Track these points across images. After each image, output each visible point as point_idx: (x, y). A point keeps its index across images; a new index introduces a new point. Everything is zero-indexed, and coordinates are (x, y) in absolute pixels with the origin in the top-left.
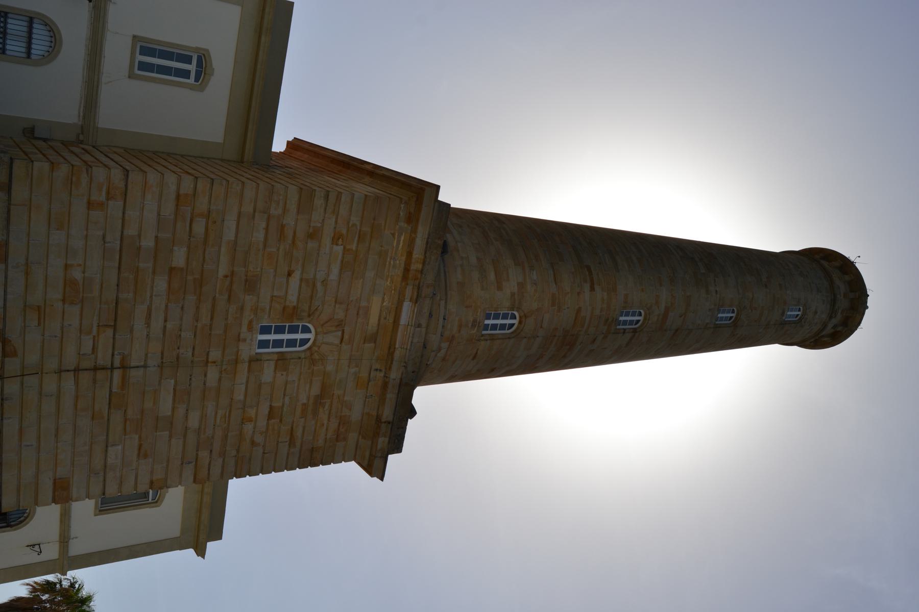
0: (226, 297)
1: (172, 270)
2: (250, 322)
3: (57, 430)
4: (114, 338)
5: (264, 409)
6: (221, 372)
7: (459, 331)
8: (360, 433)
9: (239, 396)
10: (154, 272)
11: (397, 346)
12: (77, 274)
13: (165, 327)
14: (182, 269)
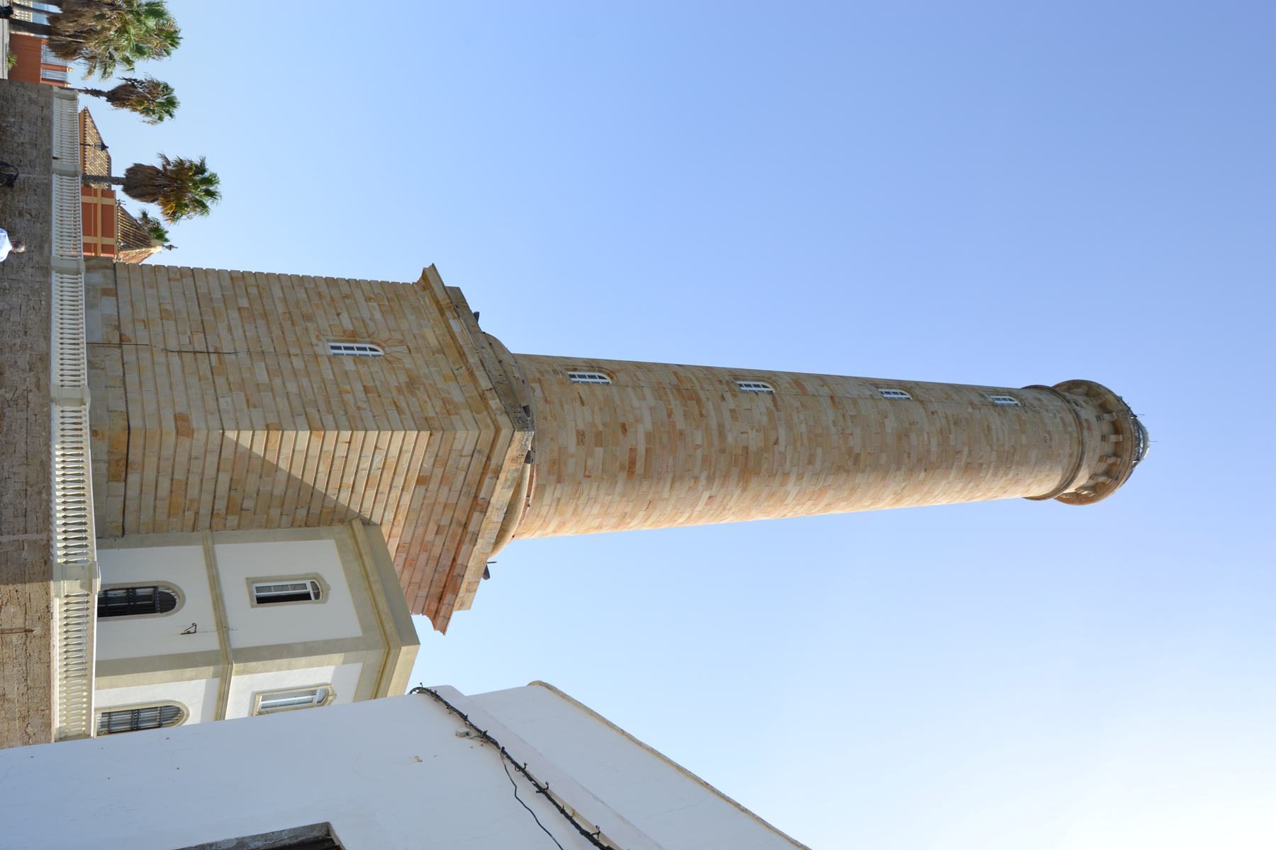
0: (290, 322)
1: (239, 309)
2: (317, 337)
3: (171, 384)
4: (205, 338)
5: (359, 388)
6: (305, 362)
7: (543, 376)
8: (472, 411)
9: (329, 375)
10: (226, 309)
11: (461, 343)
12: (169, 307)
13: (245, 336)
14: (247, 308)
